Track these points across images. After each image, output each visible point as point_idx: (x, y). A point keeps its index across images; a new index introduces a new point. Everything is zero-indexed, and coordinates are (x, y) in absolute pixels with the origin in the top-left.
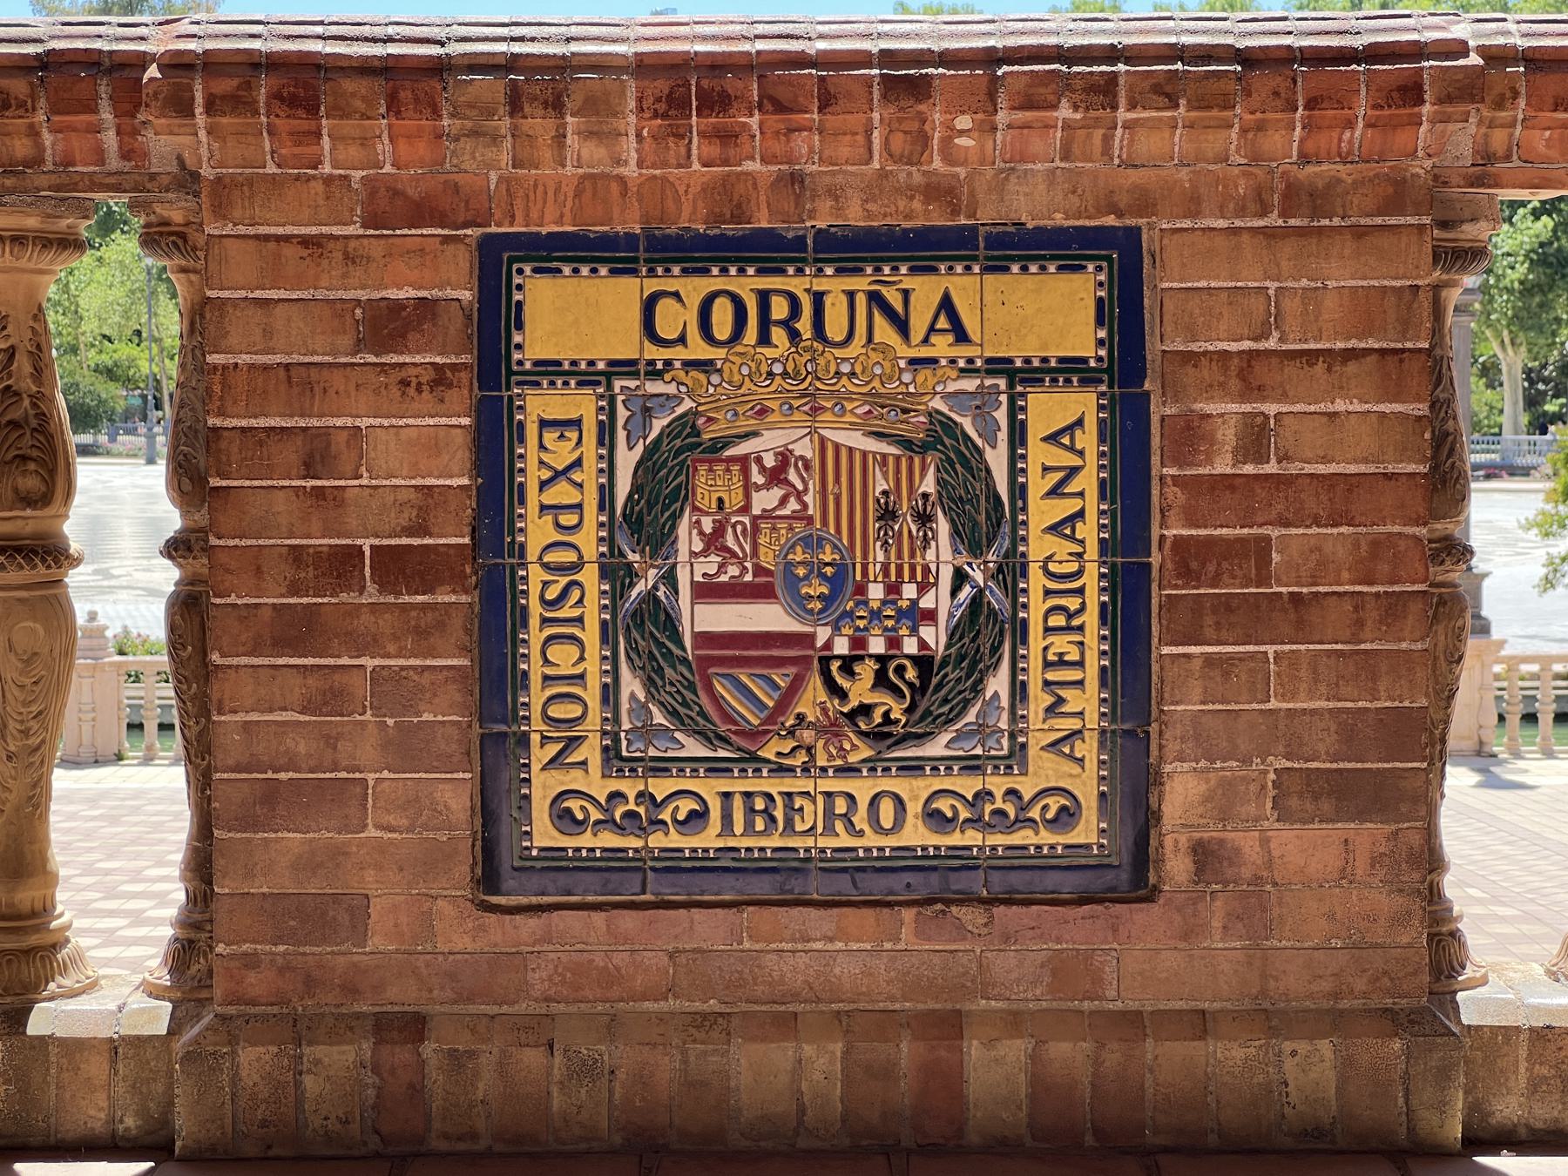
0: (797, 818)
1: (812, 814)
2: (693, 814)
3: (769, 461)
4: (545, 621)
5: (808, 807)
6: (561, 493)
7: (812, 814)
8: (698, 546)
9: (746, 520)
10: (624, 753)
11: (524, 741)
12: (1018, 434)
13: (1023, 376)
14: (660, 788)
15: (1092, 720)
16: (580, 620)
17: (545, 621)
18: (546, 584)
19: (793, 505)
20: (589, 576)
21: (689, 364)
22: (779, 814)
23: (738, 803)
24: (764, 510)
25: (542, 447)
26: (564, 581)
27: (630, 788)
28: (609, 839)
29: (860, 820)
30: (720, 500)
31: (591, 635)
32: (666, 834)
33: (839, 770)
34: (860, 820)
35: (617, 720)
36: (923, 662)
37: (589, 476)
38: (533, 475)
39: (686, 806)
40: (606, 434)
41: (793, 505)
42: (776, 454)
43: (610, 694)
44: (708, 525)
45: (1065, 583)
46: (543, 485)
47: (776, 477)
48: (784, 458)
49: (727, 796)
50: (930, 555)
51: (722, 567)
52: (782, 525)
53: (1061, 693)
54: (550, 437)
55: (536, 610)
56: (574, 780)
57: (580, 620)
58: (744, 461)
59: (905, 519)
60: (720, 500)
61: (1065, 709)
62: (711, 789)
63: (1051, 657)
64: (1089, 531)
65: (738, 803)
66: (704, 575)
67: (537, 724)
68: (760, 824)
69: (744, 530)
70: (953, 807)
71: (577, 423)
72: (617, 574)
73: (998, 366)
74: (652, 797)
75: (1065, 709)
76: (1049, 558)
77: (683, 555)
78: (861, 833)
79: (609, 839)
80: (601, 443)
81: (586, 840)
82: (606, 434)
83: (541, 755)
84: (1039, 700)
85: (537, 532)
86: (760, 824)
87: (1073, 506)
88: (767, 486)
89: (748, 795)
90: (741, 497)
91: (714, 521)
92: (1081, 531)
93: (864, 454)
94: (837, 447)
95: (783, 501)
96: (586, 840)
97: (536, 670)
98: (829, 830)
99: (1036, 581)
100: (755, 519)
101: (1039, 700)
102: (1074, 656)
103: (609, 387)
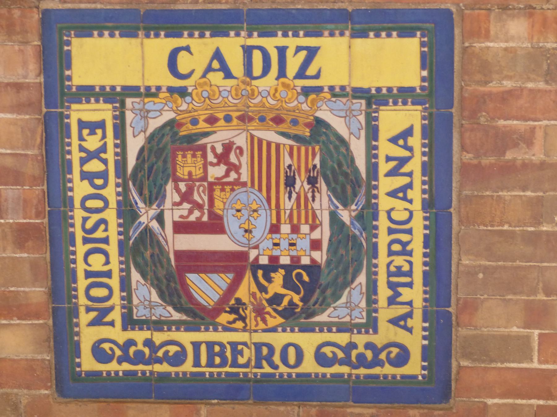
0: (239, 357)
1: (248, 354)
2: (176, 353)
3: (219, 150)
4: (86, 241)
5: (245, 349)
6: (94, 166)
7: (248, 354)
8: (177, 199)
9: (206, 184)
10: (135, 317)
11: (75, 312)
12: (373, 133)
13: (375, 99)
14: (159, 338)
15: (418, 303)
16: (106, 241)
17: (86, 241)
18: (85, 220)
19: (233, 176)
20: (111, 215)
21: (171, 90)
22: (228, 354)
23: (203, 348)
24: (217, 179)
25: (81, 138)
26: (95, 218)
27: (140, 336)
28: (126, 366)
29: (277, 359)
30: (190, 173)
31: (113, 249)
32: (161, 363)
33: (264, 331)
34: (277, 359)
35: (130, 301)
36: (313, 269)
37: (110, 156)
38: (76, 156)
39: (173, 349)
40: (120, 131)
41: (233, 176)
42: (223, 144)
43: (125, 284)
44: (182, 186)
45: (399, 227)
46: (83, 161)
47: (223, 158)
48: (228, 147)
49: (196, 345)
50: (316, 205)
51: (191, 212)
52: (228, 188)
53: (400, 290)
54: (85, 132)
55: (79, 234)
56: (104, 332)
57: (106, 241)
58: (203, 148)
59: (302, 185)
60: (190, 173)
61: (400, 299)
62: (186, 338)
63: (392, 269)
64: (416, 194)
65: (203, 348)
66: (181, 217)
67: (83, 300)
68: (218, 360)
69: (204, 192)
70: (333, 352)
71: (101, 125)
72: (128, 213)
73: (359, 93)
74: (153, 343)
75: (400, 299)
76: (392, 209)
77: (168, 204)
78: (276, 367)
79: (126, 366)
80: (116, 137)
81: (113, 366)
82: (120, 131)
83: (85, 318)
84: (384, 292)
85: (80, 189)
86: (218, 360)
87: (406, 180)
88: (218, 164)
89: (210, 345)
90: (202, 171)
91: (186, 185)
92: (410, 194)
93: (278, 146)
94: (260, 141)
95: (227, 174)
96: (113, 366)
97: (81, 267)
98: (259, 366)
99: (383, 223)
100: (211, 185)
101: (384, 292)
102: (406, 268)
103: (123, 104)
